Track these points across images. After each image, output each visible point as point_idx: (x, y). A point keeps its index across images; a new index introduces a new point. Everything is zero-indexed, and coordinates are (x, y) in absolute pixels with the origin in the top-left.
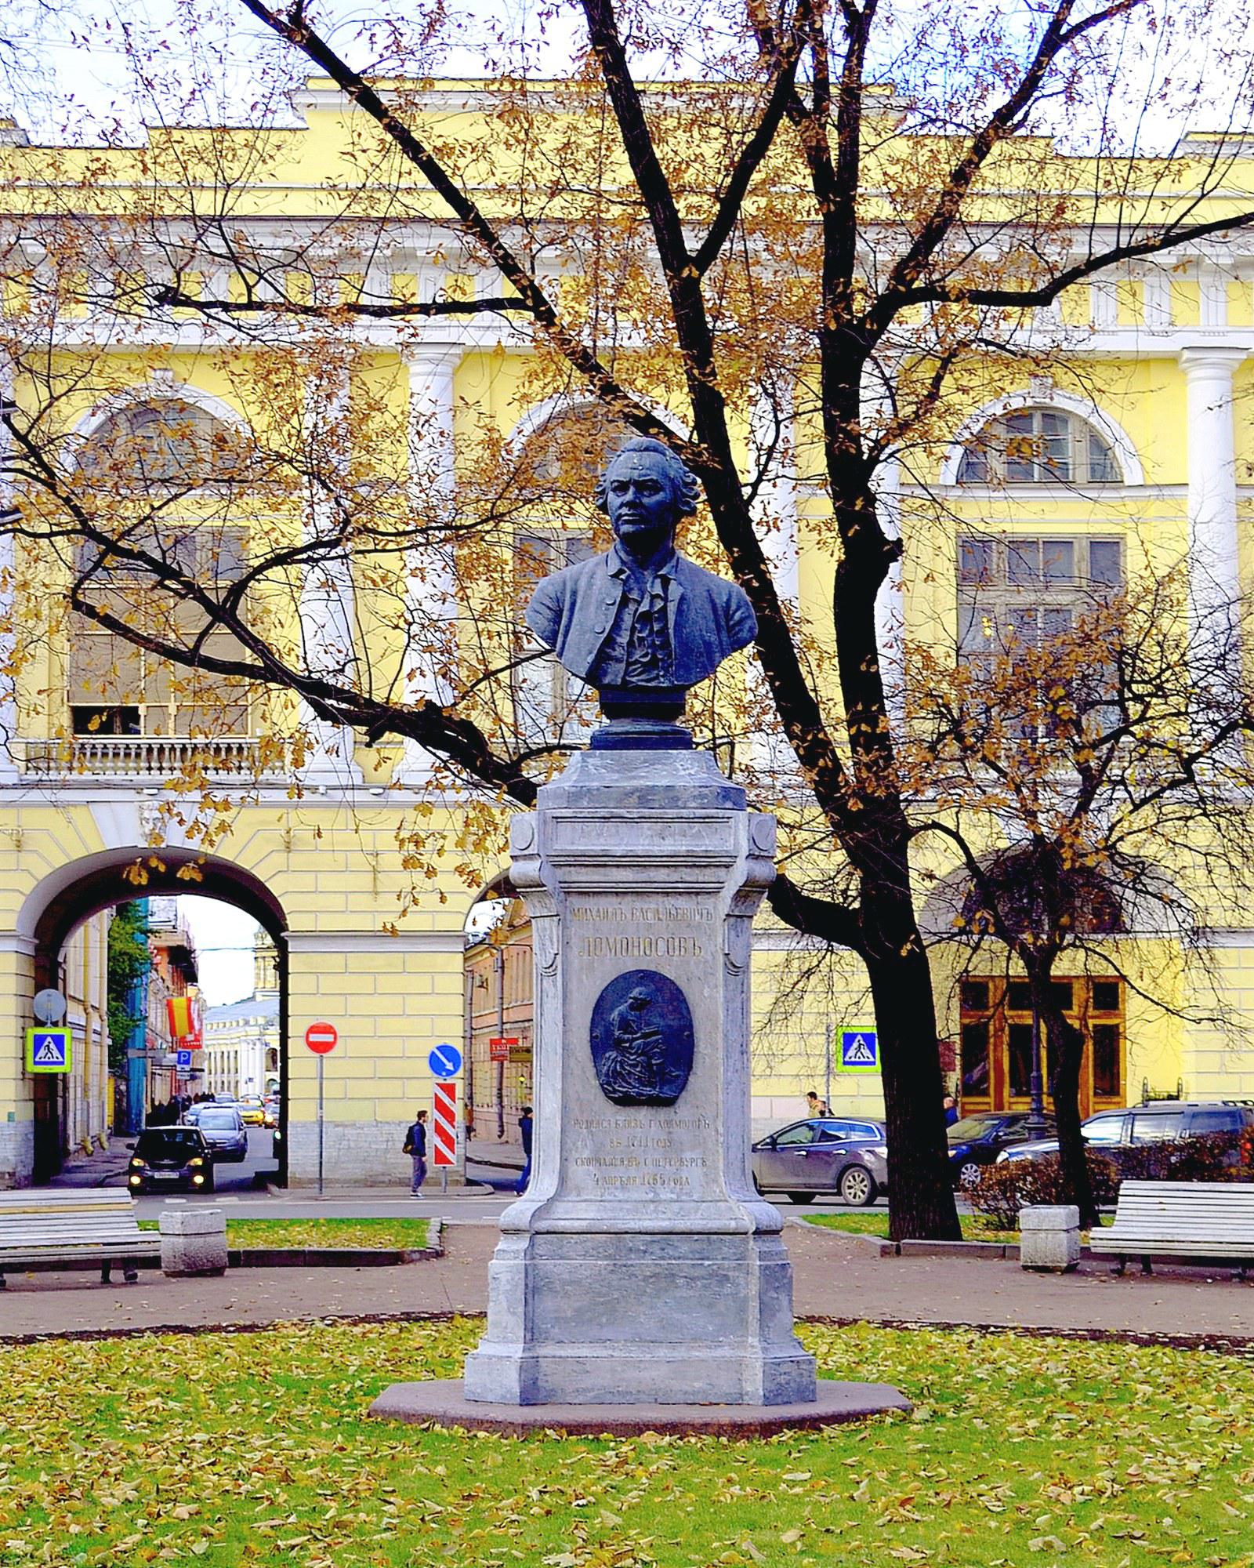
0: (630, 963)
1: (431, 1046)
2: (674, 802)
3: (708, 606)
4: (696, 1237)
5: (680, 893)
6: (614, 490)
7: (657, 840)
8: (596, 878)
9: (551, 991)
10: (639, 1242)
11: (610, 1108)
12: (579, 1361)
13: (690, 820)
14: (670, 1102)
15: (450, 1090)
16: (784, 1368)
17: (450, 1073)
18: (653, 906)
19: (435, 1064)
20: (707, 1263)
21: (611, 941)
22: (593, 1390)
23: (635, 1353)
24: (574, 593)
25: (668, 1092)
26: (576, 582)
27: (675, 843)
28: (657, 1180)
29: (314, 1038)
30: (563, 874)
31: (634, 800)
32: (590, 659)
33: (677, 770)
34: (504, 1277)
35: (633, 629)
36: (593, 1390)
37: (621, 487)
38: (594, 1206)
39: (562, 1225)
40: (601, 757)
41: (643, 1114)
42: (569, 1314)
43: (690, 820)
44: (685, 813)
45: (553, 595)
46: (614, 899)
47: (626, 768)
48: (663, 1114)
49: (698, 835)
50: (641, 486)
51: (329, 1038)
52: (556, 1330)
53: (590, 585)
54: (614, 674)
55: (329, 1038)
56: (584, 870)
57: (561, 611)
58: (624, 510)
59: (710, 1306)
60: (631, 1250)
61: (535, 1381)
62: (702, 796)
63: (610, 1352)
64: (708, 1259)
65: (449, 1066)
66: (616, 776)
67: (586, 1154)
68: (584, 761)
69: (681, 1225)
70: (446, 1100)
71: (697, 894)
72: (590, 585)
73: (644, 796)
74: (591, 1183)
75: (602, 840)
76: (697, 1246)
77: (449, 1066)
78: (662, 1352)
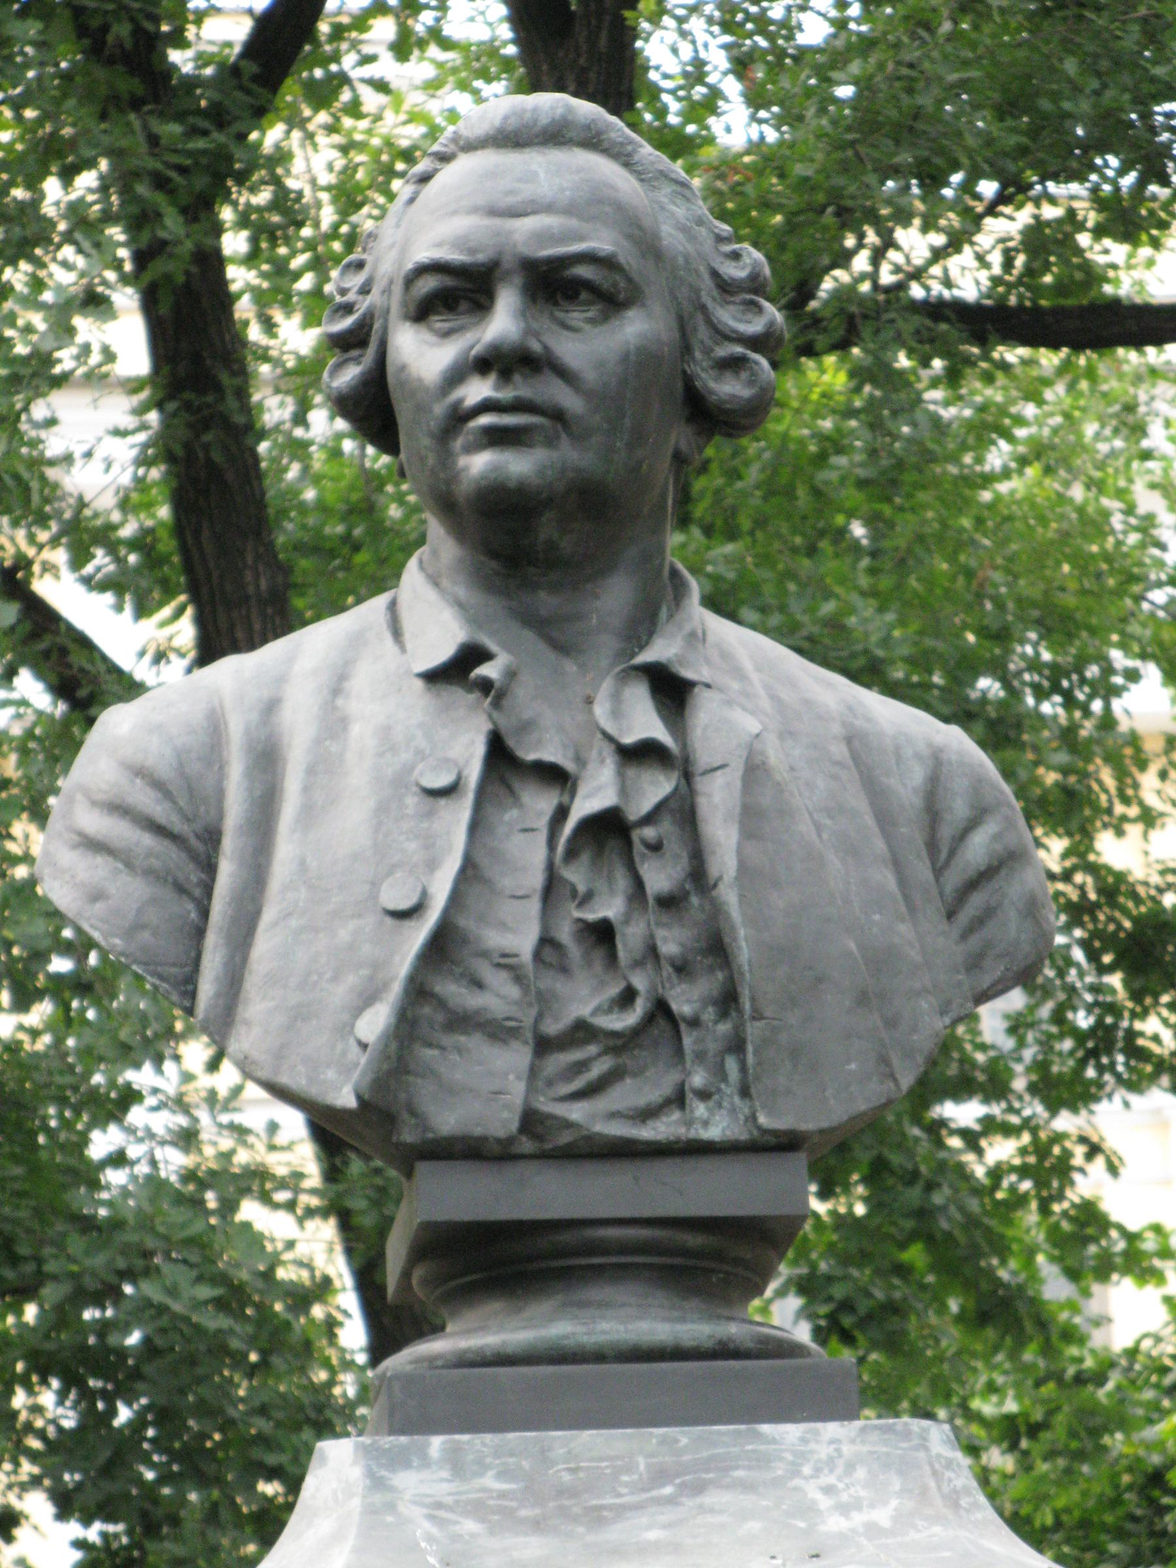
3: (859, 802)
6: (422, 313)
24: (267, 759)
26: (271, 707)
32: (374, 1023)
33: (809, 1510)
35: (552, 888)
37: (454, 291)
40: (456, 1463)
45: (165, 771)
50: (553, 283)
53: (334, 723)
54: (484, 1087)
57: (213, 837)
58: (477, 390)
68: (377, 1483)
72: (334, 723)
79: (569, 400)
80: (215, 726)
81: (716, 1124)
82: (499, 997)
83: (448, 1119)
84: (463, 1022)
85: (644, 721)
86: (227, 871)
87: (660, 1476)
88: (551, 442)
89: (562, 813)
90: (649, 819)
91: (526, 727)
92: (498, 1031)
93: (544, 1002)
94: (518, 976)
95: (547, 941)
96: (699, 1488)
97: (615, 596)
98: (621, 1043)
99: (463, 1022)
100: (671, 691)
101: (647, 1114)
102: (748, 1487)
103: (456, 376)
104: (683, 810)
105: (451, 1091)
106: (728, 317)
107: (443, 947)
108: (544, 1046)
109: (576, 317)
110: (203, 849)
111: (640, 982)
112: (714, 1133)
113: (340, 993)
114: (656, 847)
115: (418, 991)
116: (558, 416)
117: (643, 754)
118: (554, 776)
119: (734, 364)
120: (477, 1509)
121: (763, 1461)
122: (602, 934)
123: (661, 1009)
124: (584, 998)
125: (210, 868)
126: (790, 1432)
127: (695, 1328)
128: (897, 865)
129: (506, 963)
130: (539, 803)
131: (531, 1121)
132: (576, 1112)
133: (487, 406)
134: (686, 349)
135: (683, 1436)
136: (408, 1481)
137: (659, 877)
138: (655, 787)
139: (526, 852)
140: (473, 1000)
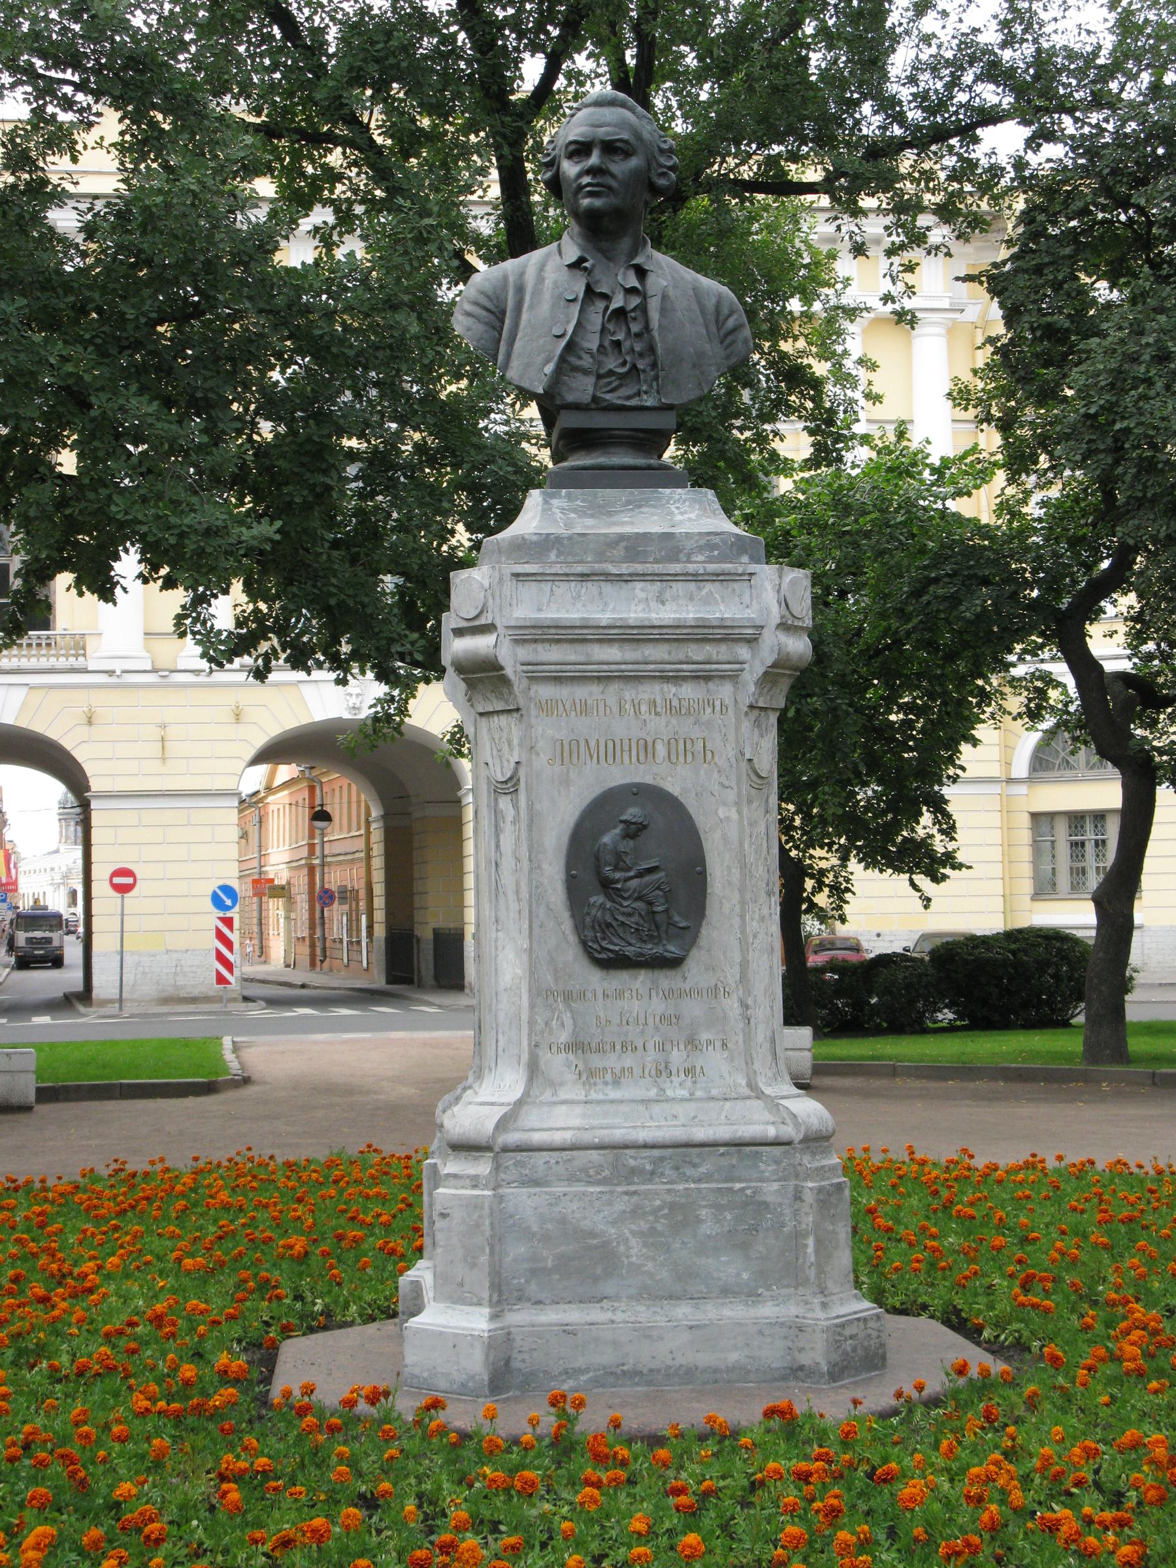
0: (619, 775)
1: (213, 886)
2: (673, 557)
3: (695, 307)
4: (722, 1150)
5: (684, 678)
6: (570, 156)
7: (653, 604)
8: (573, 658)
9: (510, 813)
10: (643, 1160)
12: (568, 1331)
13: (696, 578)
14: (674, 963)
15: (228, 922)
16: (848, 1332)
17: (228, 908)
18: (646, 696)
19: (217, 901)
20: (738, 1186)
21: (592, 744)
22: (587, 1370)
23: (643, 1313)
24: (520, 290)
25: (673, 949)
26: (522, 274)
27: (677, 608)
28: (664, 1070)
29: (117, 880)
30: (524, 653)
31: (619, 552)
32: (549, 368)
33: (672, 513)
34: (457, 1215)
35: (603, 330)
36: (587, 1370)
37: (580, 150)
38: (578, 1110)
39: (537, 1138)
40: (569, 498)
41: (640, 980)
42: (550, 1264)
43: (696, 578)
44: (691, 568)
45: (490, 293)
46: (595, 689)
47: (602, 511)
48: (666, 979)
49: (708, 601)
50: (610, 148)
51: (129, 880)
52: (533, 1286)
53: (540, 279)
54: (582, 388)
55: (129, 880)
56: (554, 647)
57: (504, 312)
58: (586, 180)
59: (745, 1247)
60: (633, 1171)
61: (507, 1362)
62: (711, 547)
63: (609, 1315)
64: (740, 1180)
65: (229, 902)
66: (590, 522)
67: (564, 1037)
68: (546, 502)
69: (701, 1134)
70: (225, 930)
71: (707, 678)
72: (540, 279)
73: (635, 546)
74: (570, 1077)
75: (579, 605)
76: (724, 1162)
77: (229, 902)
78: (683, 1311)
79: (614, 184)
80: (505, 279)
81: (649, 402)
82: (586, 362)
83: (570, 398)
84: (576, 369)
85: (632, 281)
86: (507, 322)
87: (628, 503)
88: (608, 196)
89: (607, 308)
90: (633, 310)
91: (597, 282)
92: (586, 372)
93: (600, 364)
94: (592, 356)
95: (601, 346)
96: (640, 507)
97: (625, 243)
98: (622, 376)
99: (576, 369)
100: (641, 273)
101: (629, 398)
102: (654, 507)
103: (580, 175)
104: (643, 308)
105: (571, 389)
106: (662, 160)
107: (570, 347)
108: (599, 377)
109: (616, 158)
110: (500, 315)
111: (628, 358)
112: (648, 404)
113: (540, 360)
114: (635, 319)
115: (562, 359)
116: (610, 188)
117: (632, 291)
118: (606, 297)
119: (663, 175)
120: (575, 511)
121: (659, 499)
122: (617, 344)
123: (634, 367)
124: (612, 363)
125: (503, 322)
126: (668, 491)
127: (640, 461)
128: (707, 327)
129: (589, 352)
130: (600, 305)
131: (595, 399)
132: (608, 397)
133: (588, 185)
134: (649, 170)
135: (636, 491)
136: (555, 502)
137: (635, 328)
138: (635, 301)
139: (596, 319)
140: (578, 363)
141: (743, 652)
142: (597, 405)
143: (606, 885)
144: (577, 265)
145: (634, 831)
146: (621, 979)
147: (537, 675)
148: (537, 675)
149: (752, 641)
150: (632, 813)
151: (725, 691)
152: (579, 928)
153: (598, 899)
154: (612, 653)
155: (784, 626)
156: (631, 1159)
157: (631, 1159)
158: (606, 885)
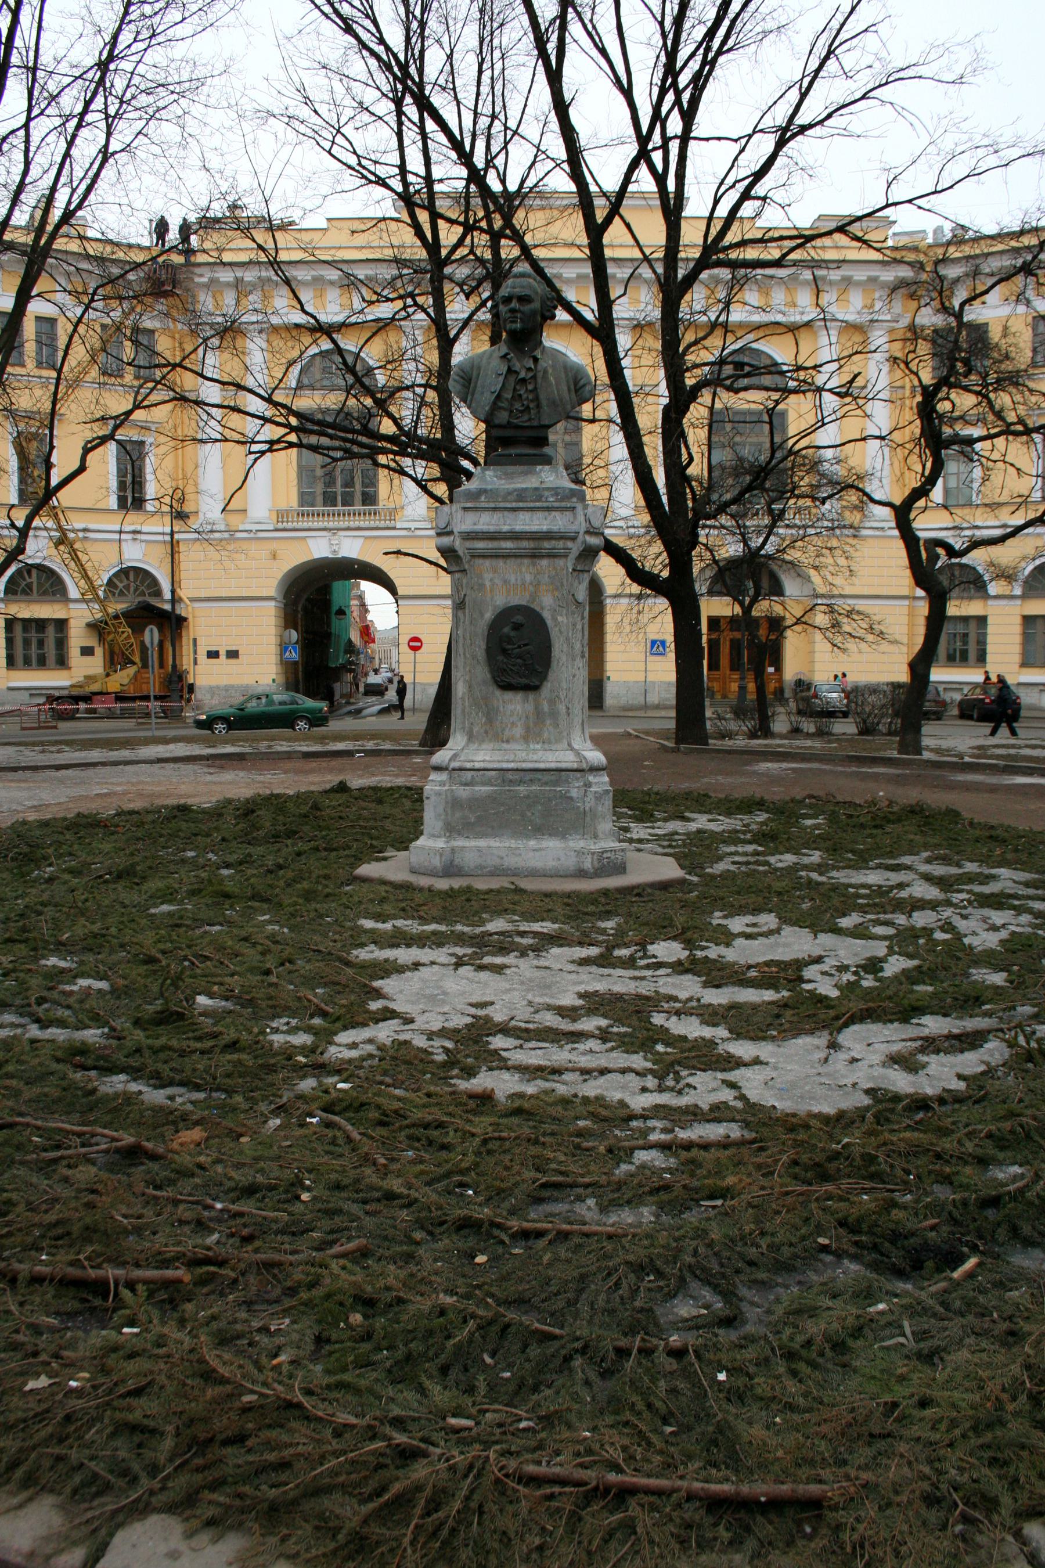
2: (539, 499)
10: (516, 776)
11: (498, 693)
14: (535, 688)
30: (469, 544)
43: (548, 509)
47: (508, 476)
48: (531, 696)
54: (503, 417)
73: (521, 495)
82: (505, 405)
104: (534, 377)
107: (499, 397)
110: (469, 381)
115: (494, 403)
137: (530, 387)
141: (570, 544)
142: (509, 425)
143: (504, 651)
144: (504, 357)
145: (517, 627)
146: (509, 695)
147: (475, 555)
148: (475, 555)
149: (573, 539)
150: (519, 618)
151: (561, 562)
152: (492, 672)
153: (500, 658)
154: (509, 544)
155: (587, 532)
156: (510, 776)
157: (510, 776)
158: (504, 651)
